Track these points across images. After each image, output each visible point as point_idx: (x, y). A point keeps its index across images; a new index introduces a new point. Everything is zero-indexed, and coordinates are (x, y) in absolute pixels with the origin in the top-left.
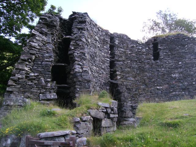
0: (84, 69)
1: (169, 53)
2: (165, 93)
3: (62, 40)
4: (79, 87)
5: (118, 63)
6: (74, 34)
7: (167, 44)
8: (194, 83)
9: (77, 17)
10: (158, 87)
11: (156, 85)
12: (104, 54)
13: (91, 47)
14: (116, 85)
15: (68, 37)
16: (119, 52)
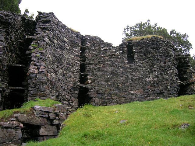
0: (40, 70)
1: (144, 57)
2: (139, 97)
3: (24, 40)
4: (32, 89)
5: (90, 66)
6: (37, 34)
7: (142, 47)
8: (169, 87)
9: (42, 16)
10: (132, 92)
11: (130, 89)
12: (73, 57)
13: (57, 48)
14: (87, 90)
15: (30, 37)
16: (90, 55)
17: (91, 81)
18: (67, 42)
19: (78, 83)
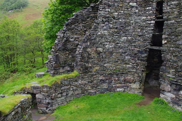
17: (166, 41)
18: (135, 5)
19: (148, 45)
